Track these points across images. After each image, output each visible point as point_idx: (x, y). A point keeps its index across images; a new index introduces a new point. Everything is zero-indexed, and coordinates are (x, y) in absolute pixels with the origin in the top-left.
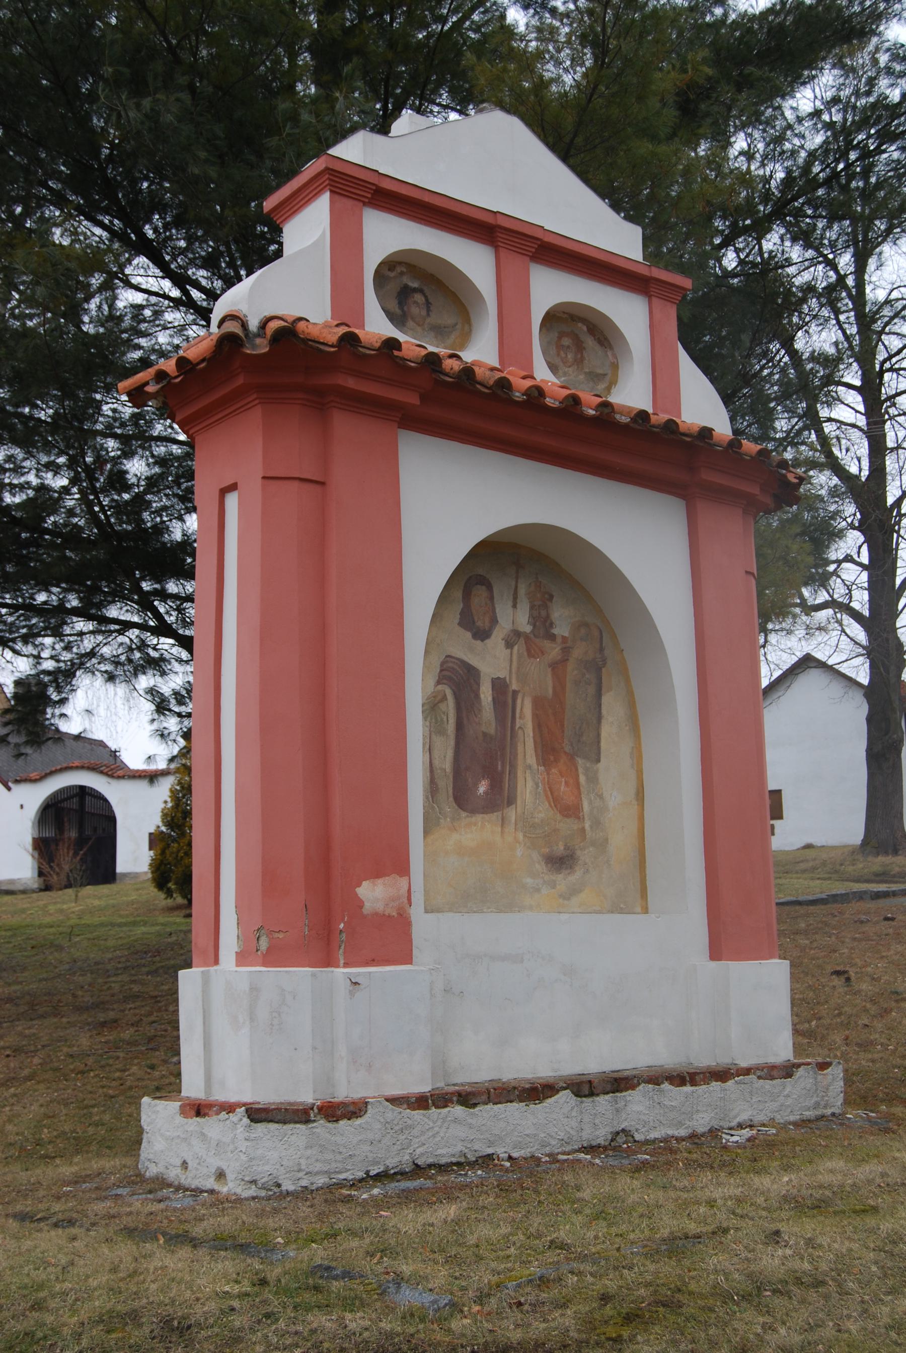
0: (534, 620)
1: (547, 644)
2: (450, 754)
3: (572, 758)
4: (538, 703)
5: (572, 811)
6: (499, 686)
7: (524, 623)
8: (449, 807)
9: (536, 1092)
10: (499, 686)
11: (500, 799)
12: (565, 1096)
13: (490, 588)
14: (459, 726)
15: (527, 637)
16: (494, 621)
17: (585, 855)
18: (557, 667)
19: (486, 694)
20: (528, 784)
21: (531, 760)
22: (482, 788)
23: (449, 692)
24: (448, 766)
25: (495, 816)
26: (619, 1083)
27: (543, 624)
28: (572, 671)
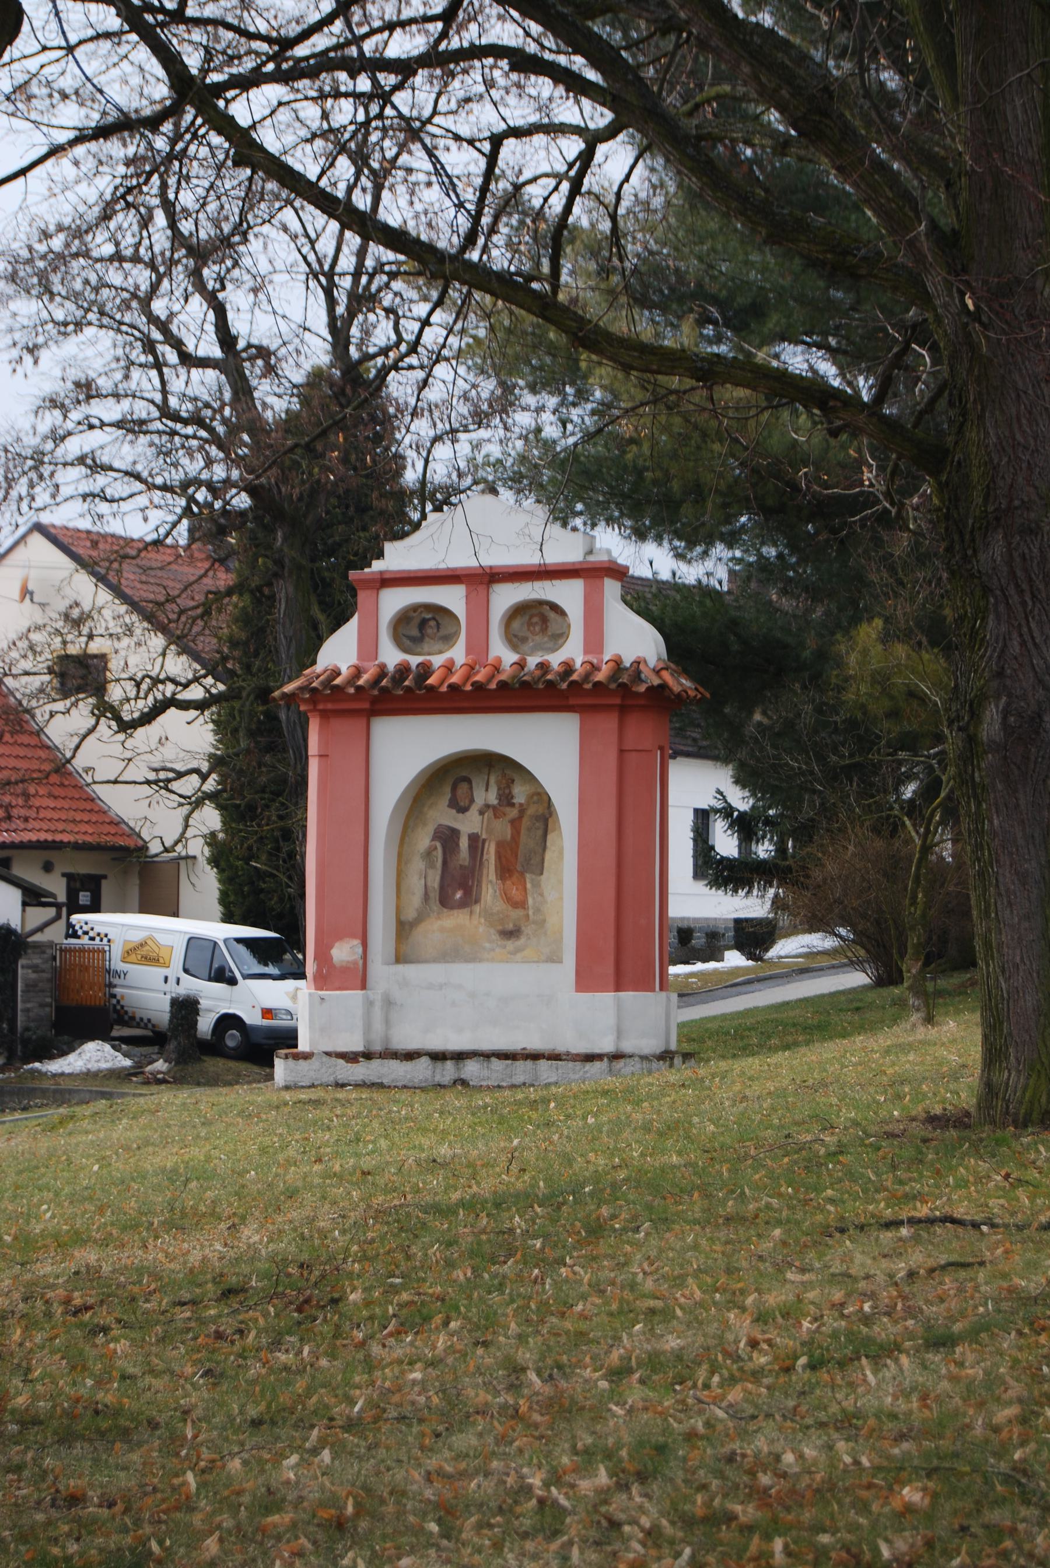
0: (500, 797)
1: (508, 809)
2: (438, 878)
3: (522, 874)
4: (500, 845)
5: (521, 904)
6: (474, 838)
7: (492, 798)
8: (435, 906)
9: (410, 1056)
10: (474, 838)
11: (470, 899)
12: (425, 1061)
13: (470, 782)
14: (445, 863)
15: (494, 808)
16: (472, 801)
17: (528, 930)
18: (515, 823)
19: (464, 843)
20: (490, 891)
21: (492, 876)
22: (459, 895)
23: (438, 845)
24: (436, 885)
25: (467, 910)
26: (460, 1057)
27: (506, 799)
28: (526, 822)
